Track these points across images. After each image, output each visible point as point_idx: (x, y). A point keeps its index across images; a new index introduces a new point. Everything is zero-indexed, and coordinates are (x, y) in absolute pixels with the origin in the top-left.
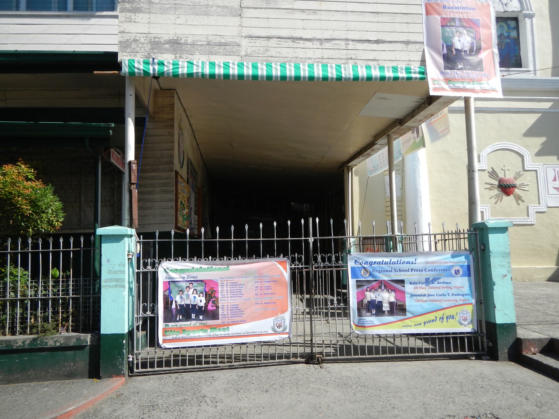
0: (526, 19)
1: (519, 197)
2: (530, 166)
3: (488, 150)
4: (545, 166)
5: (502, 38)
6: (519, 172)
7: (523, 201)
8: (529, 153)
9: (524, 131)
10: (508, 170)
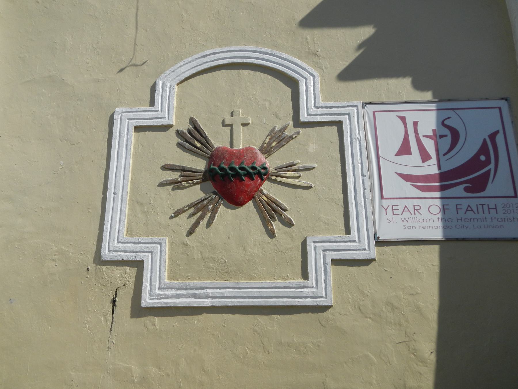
1: (275, 211)
2: (319, 111)
3: (182, 70)
4: (370, 109)
6: (282, 131)
7: (289, 224)
10: (245, 125)
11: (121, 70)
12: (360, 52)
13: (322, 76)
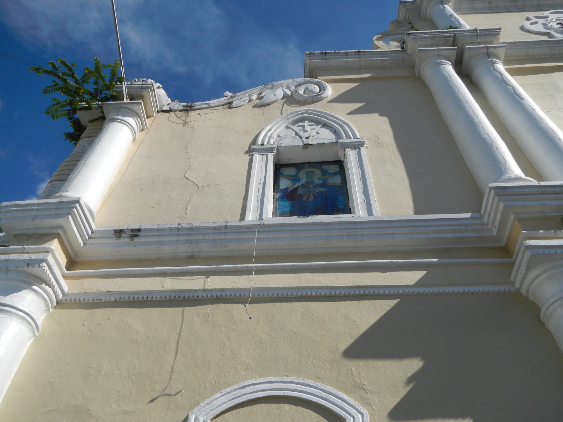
0: (346, 149)
3: (218, 402)
5: (311, 186)
8: (365, 411)
9: (346, 342)
11: (153, 400)
12: (410, 387)
13: (371, 414)
